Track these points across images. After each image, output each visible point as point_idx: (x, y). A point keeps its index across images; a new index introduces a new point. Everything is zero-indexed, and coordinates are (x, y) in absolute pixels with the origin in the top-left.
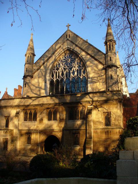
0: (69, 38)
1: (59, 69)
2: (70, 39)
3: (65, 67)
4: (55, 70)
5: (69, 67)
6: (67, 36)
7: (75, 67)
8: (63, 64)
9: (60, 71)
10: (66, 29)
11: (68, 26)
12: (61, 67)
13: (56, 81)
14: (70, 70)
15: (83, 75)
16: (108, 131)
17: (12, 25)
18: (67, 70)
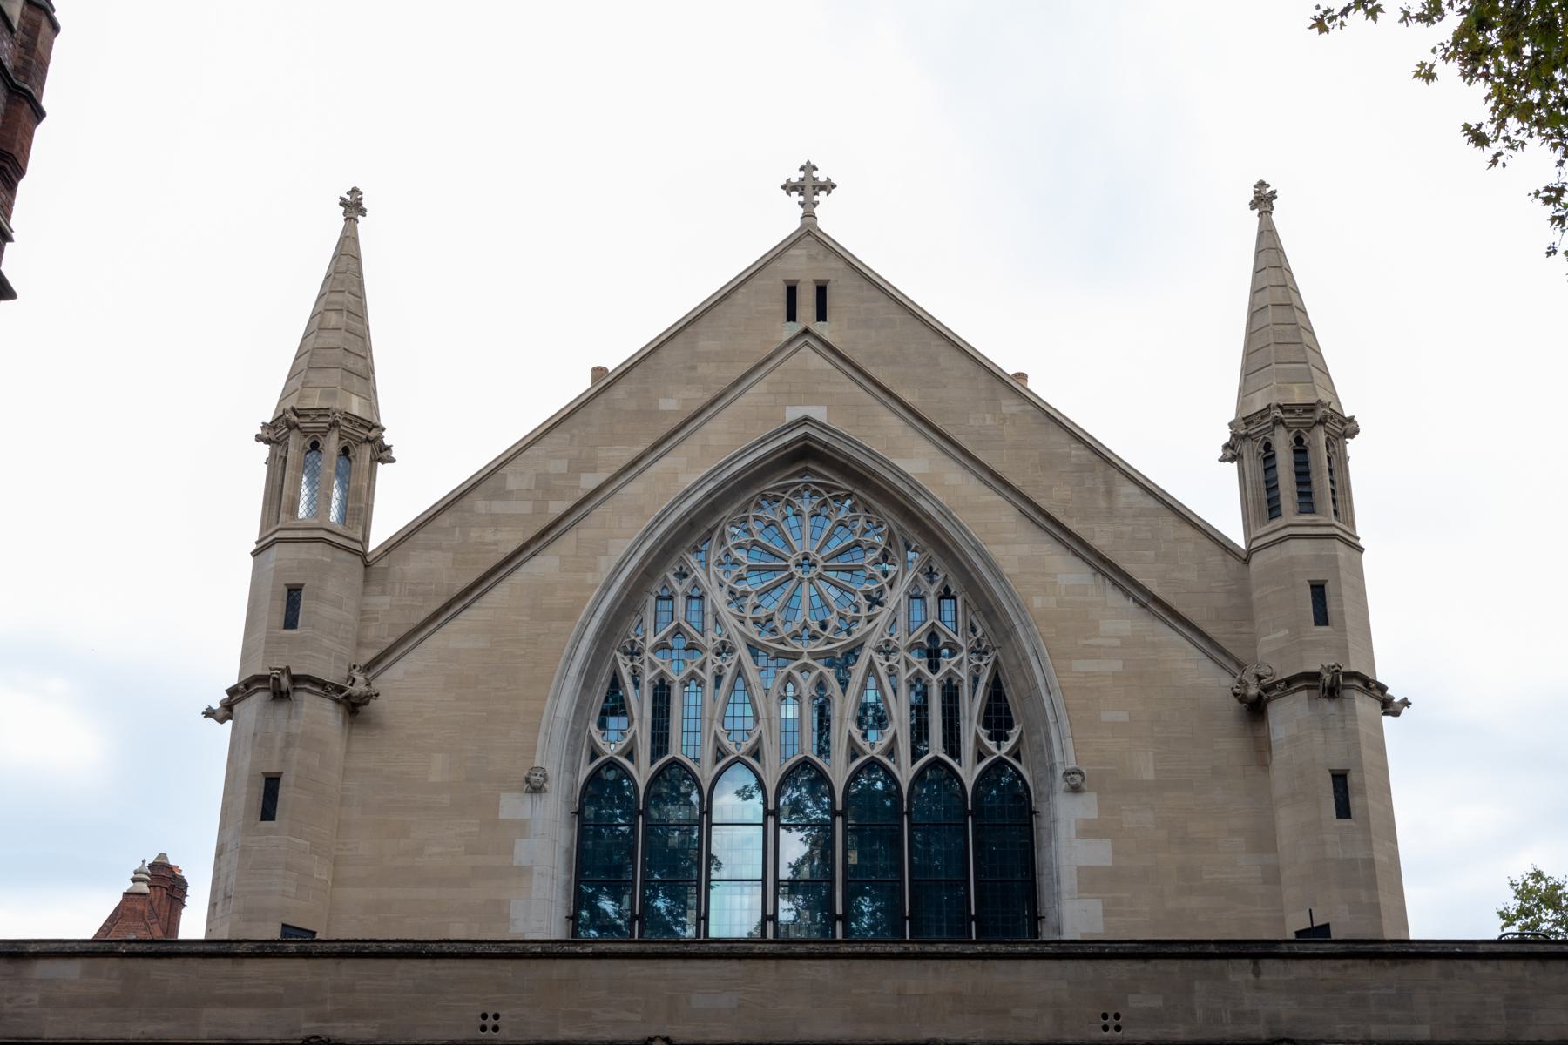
0: (822, 315)
4: (648, 654)
6: (792, 292)
7: (886, 650)
8: (736, 597)
10: (786, 218)
11: (809, 186)
14: (830, 674)
15: (991, 745)
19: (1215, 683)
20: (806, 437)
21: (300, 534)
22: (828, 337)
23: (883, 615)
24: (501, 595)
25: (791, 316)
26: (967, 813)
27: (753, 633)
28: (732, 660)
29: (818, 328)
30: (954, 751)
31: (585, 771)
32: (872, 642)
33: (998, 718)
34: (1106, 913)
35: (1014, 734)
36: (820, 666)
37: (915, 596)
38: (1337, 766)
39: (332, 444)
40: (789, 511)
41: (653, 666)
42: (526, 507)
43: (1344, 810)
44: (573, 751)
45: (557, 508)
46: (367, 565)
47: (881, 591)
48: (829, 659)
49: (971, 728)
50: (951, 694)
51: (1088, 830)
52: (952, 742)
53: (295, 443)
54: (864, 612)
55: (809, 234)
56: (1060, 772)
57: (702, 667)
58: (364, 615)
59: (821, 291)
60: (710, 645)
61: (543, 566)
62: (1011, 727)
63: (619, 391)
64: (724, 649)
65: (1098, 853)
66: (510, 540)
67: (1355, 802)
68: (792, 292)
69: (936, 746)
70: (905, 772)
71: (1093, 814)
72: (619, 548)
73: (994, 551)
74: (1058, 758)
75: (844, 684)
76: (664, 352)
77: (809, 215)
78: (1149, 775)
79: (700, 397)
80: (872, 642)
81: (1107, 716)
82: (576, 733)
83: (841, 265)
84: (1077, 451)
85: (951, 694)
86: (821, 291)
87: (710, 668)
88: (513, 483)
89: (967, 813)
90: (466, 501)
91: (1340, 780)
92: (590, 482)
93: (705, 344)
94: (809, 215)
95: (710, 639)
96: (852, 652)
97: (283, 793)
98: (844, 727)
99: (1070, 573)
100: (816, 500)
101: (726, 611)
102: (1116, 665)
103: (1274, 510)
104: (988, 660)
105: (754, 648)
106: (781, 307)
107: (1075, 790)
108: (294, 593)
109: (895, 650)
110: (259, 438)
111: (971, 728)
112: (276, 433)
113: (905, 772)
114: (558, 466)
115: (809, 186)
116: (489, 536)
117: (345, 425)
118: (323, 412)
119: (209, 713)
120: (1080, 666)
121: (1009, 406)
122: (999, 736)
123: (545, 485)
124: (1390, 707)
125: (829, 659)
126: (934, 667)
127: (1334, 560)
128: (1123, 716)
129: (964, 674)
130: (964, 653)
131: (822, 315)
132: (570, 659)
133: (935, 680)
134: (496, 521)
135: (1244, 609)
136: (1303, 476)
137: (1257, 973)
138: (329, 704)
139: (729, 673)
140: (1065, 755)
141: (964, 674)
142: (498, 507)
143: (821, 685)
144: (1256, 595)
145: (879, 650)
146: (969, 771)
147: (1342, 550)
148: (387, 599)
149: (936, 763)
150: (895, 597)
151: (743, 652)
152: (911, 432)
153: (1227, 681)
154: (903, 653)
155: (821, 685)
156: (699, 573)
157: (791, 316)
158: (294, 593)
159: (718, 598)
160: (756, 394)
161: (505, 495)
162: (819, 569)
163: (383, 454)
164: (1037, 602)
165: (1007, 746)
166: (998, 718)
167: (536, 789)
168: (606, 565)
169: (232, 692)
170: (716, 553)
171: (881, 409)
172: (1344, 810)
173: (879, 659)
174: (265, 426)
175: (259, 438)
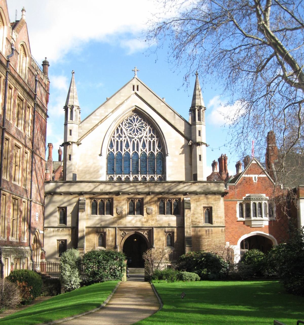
0: (138, 90)
1: (121, 137)
2: (138, 92)
3: (131, 136)
5: (137, 136)
6: (134, 86)
7: (146, 137)
8: (127, 130)
12: (124, 134)
13: (117, 154)
14: (138, 140)
16: (209, 230)
17: (231, 154)
18: (134, 139)
25: (134, 90)
27: (129, 135)
31: (108, 153)
37: (150, 130)
42: (98, 117)
45: (103, 118)
52: (154, 150)
59: (138, 86)
64: (125, 137)
66: (97, 122)
68: (134, 86)
79: (121, 102)
86: (138, 86)
87: (123, 140)
93: (122, 94)
95: (123, 136)
96: (141, 138)
101: (125, 132)
110: (63, 108)
111: (156, 147)
114: (103, 112)
127: (201, 128)
131: (138, 90)
142: (95, 117)
143: (137, 142)
148: (82, 130)
151: (127, 137)
155: (137, 142)
157: (134, 90)
159: (124, 130)
161: (96, 116)
169: (63, 143)
174: (64, 107)
175: (63, 108)
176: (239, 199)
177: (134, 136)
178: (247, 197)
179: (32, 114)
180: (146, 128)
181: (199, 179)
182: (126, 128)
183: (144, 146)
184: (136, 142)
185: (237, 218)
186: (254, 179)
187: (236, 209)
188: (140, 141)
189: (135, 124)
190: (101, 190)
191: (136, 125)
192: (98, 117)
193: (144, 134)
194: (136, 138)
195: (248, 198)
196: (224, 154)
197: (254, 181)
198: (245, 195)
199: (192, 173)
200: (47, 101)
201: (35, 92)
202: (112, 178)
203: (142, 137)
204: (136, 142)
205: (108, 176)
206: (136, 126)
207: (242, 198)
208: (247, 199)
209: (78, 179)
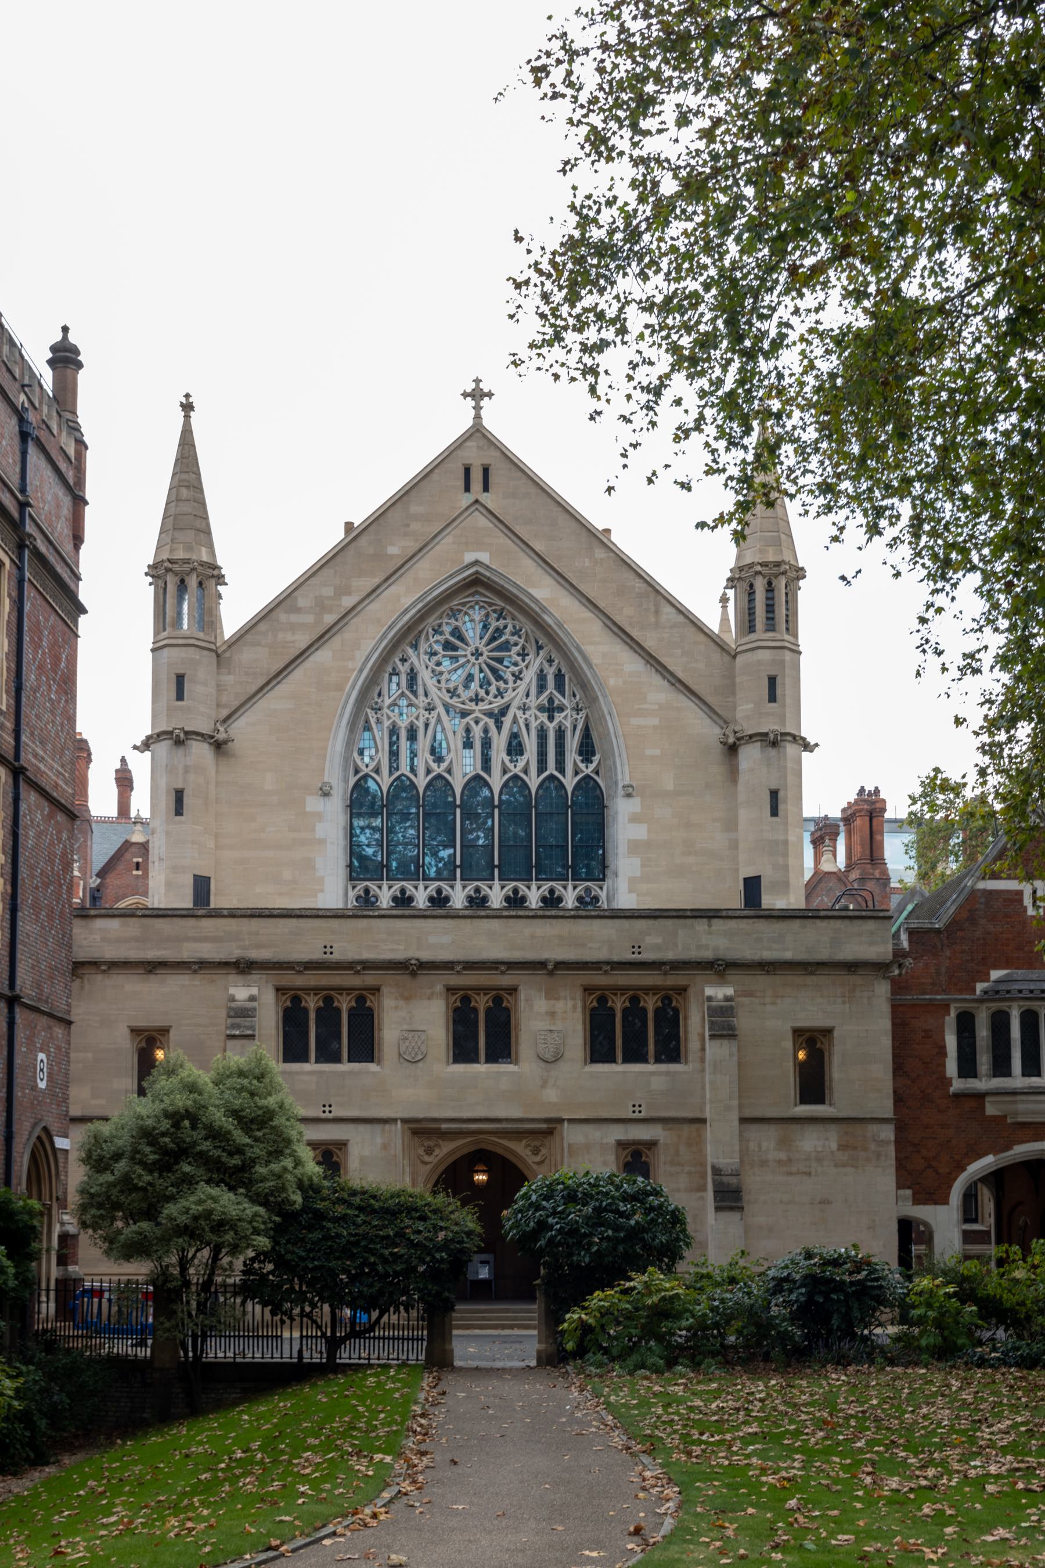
4: (385, 710)
5: (484, 706)
7: (524, 708)
9: (420, 724)
14: (491, 723)
15: (582, 766)
19: (710, 732)
20: (477, 572)
21: (180, 642)
22: (490, 506)
23: (522, 686)
24: (298, 674)
26: (568, 807)
27: (447, 697)
28: (434, 714)
29: (484, 498)
30: (562, 770)
31: (352, 781)
32: (516, 703)
33: (587, 750)
34: (642, 866)
35: (596, 759)
36: (486, 719)
38: (773, 787)
39: (192, 582)
40: (467, 618)
41: (389, 718)
42: (309, 619)
43: (774, 812)
44: (345, 769)
45: (329, 619)
46: (218, 656)
47: (521, 672)
48: (489, 714)
49: (572, 757)
50: (560, 734)
51: (634, 819)
52: (561, 767)
53: (172, 581)
54: (511, 685)
55: (478, 432)
56: (620, 785)
57: (417, 718)
58: (220, 688)
59: (486, 471)
60: (422, 705)
61: (322, 656)
62: (594, 754)
63: (363, 541)
65: (640, 832)
66: (303, 640)
67: (781, 807)
69: (551, 769)
70: (534, 782)
71: (638, 810)
72: (368, 645)
73: (588, 649)
74: (620, 777)
75: (499, 726)
76: (390, 514)
77: (478, 417)
78: (670, 787)
79: (413, 545)
80: (516, 703)
81: (649, 752)
82: (347, 759)
83: (498, 454)
84: (639, 585)
85: (560, 734)
86: (486, 471)
87: (422, 719)
88: (302, 602)
89: (568, 807)
90: (274, 613)
91: (774, 794)
92: (348, 602)
94: (478, 417)
96: (504, 711)
97: (186, 800)
98: (499, 754)
99: (632, 664)
100: (483, 612)
101: (431, 683)
102: (655, 721)
103: (752, 629)
104: (583, 714)
105: (447, 707)
106: (461, 483)
107: (629, 795)
108: (180, 679)
109: (529, 708)
110: (147, 574)
111: (572, 757)
112: (158, 572)
113: (534, 782)
114: (328, 591)
115: (478, 395)
116: (289, 637)
117: (200, 569)
118: (187, 561)
119: (135, 747)
120: (635, 721)
121: (600, 553)
122: (587, 760)
123: (321, 605)
124: (808, 747)
125: (489, 714)
126: (551, 718)
127: (782, 663)
128: (657, 752)
129: (568, 724)
130: (568, 711)
132: (342, 716)
133: (551, 727)
134: (293, 627)
135: (730, 688)
136: (770, 608)
137: (710, 926)
138: (206, 746)
139: (433, 722)
140: (624, 775)
141: (568, 724)
142: (294, 618)
143: (486, 731)
144: (738, 680)
145: (519, 708)
146: (569, 782)
147: (788, 656)
148: (231, 678)
149: (551, 777)
150: (530, 676)
151: (441, 709)
152: (540, 571)
153: (717, 731)
154: (534, 711)
155: (486, 731)
156: (414, 659)
158: (180, 679)
159: (425, 676)
160: (446, 544)
161: (298, 610)
162: (484, 657)
163: (220, 579)
164: (612, 682)
165: (592, 767)
166: (587, 750)
167: (326, 794)
168: (360, 656)
169: (148, 738)
170: (423, 647)
171: (522, 554)
172: (774, 812)
173: (519, 713)
175: (147, 574)
176: (961, 991)
177: (472, 706)
178: (996, 982)
179: (9, 595)
180: (527, 667)
181: (769, 901)
182: (431, 664)
183: (515, 748)
184: (477, 732)
185: (949, 1082)
186: (1027, 901)
187: (944, 1040)
188: (499, 726)
189: (477, 650)
190: (328, 950)
191: (477, 654)
192: (309, 619)
193: (515, 696)
194: (477, 714)
195: (1002, 987)
196: (870, 787)
197: (1031, 912)
198: (988, 974)
199: (737, 870)
200: (78, 539)
201: (23, 490)
202: (367, 900)
203: (508, 707)
204: (477, 732)
205: (354, 888)
206: (481, 659)
207: (974, 990)
208: (997, 992)
209: (216, 902)
